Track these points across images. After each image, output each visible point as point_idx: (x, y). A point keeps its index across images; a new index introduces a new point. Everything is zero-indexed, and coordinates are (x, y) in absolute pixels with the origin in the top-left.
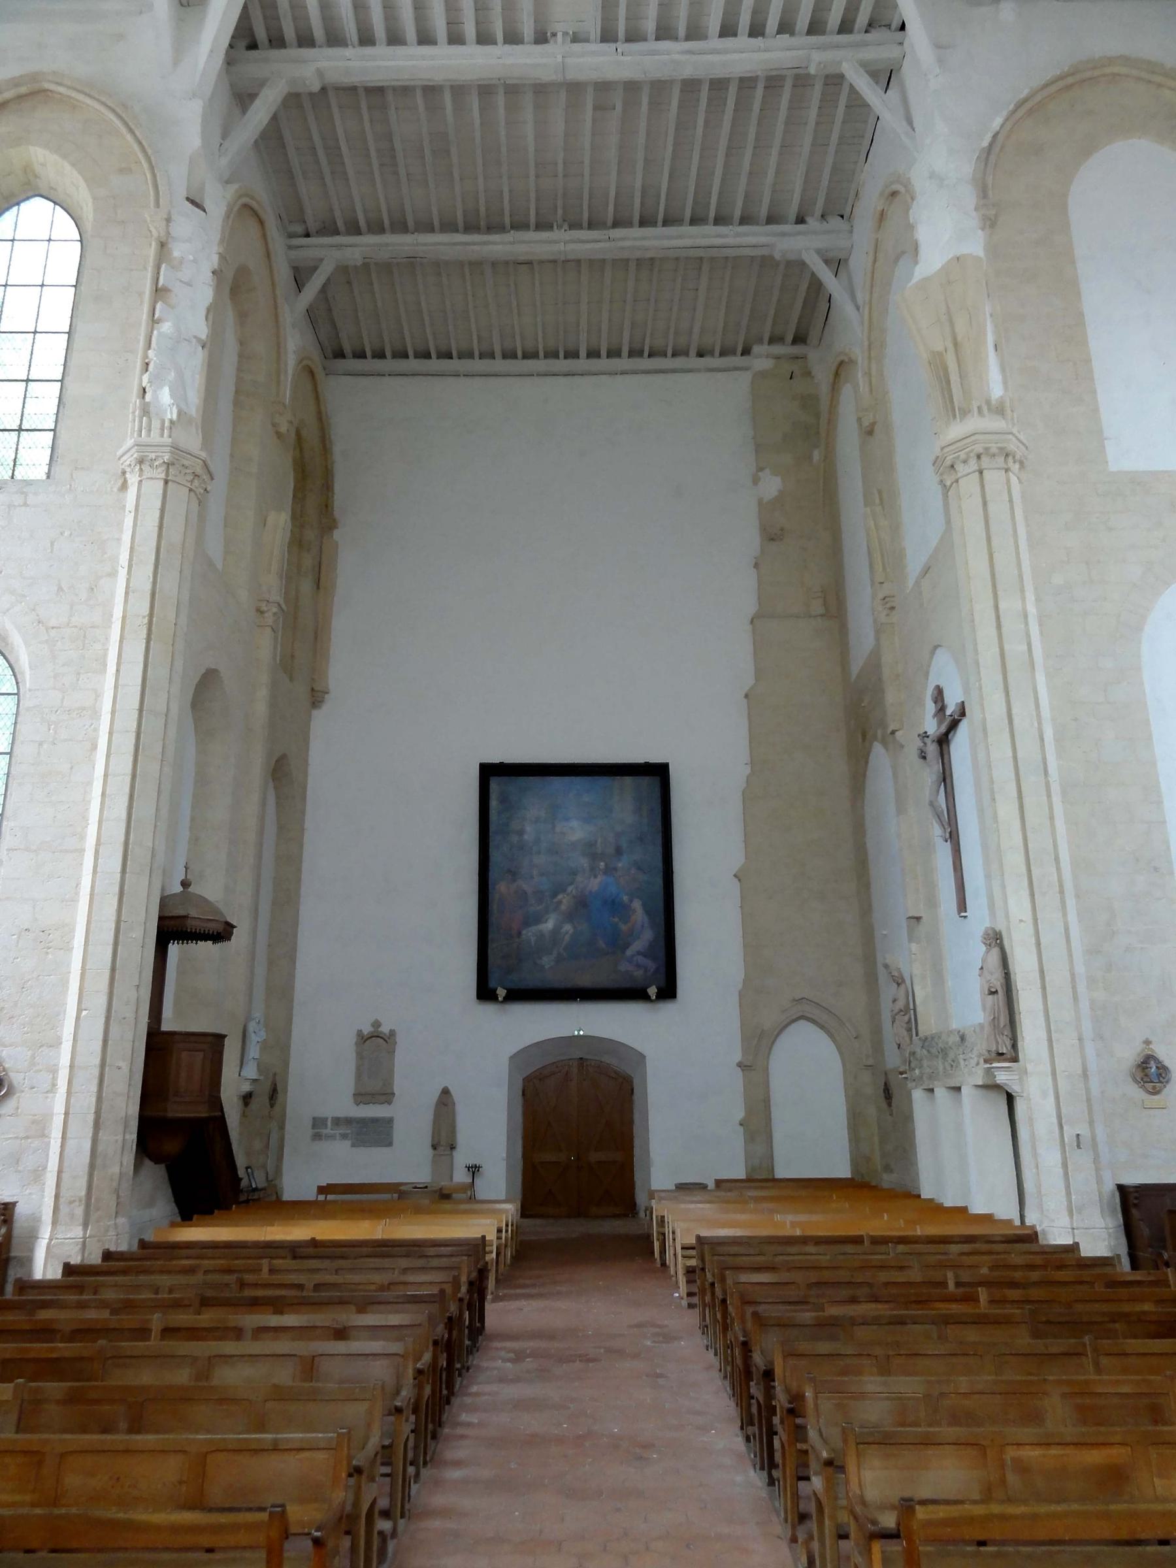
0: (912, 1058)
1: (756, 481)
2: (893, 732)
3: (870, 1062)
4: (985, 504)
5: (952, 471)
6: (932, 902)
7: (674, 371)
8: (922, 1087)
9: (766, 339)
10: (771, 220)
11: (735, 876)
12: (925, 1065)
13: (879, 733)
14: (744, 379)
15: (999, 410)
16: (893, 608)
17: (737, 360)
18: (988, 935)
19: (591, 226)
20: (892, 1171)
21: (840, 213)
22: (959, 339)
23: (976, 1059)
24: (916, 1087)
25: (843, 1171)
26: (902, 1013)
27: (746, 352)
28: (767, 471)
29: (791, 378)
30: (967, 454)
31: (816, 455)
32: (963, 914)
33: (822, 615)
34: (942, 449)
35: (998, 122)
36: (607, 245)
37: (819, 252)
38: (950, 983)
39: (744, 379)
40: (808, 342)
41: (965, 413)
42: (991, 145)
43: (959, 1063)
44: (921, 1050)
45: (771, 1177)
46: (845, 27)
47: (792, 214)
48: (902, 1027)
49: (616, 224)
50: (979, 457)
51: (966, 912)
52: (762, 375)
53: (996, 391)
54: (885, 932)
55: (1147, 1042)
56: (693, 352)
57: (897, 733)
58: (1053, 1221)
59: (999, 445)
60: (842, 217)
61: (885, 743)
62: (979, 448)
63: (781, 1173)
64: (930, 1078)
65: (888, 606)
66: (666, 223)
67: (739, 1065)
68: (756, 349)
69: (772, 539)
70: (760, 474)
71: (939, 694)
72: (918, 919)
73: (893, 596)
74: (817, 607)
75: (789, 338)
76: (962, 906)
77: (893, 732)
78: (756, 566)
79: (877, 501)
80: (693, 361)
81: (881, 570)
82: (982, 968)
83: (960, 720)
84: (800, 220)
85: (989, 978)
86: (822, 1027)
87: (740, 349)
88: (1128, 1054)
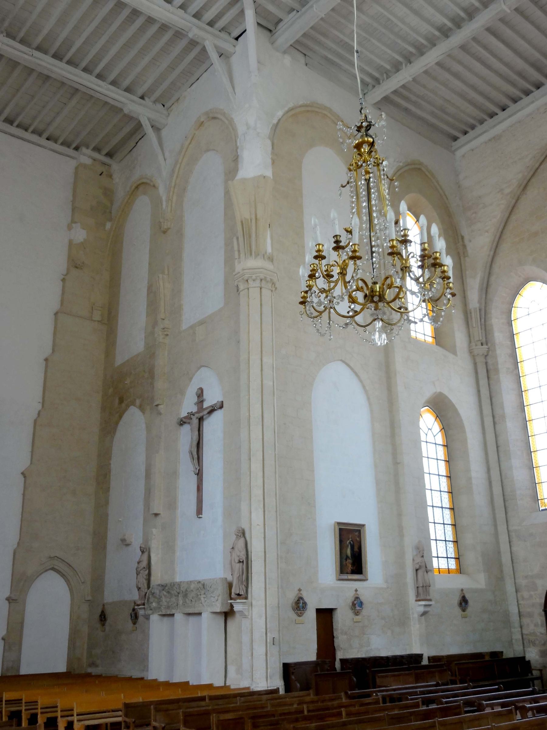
0: (151, 596)
1: (70, 228)
2: (157, 405)
3: (90, 598)
4: (261, 305)
5: (246, 283)
6: (172, 505)
7: (29, 141)
8: (160, 613)
9: (91, 147)
10: (128, 90)
11: (23, 473)
12: (164, 600)
13: (138, 402)
14: (73, 163)
15: (271, 259)
16: (167, 335)
17: (70, 151)
18: (240, 530)
19: (22, 42)
20: (97, 666)
21: (164, 104)
22: (258, 217)
23: (216, 597)
24: (153, 613)
25: (62, 668)
26: (145, 570)
27: (77, 149)
28: (79, 225)
29: (100, 175)
30: (256, 277)
31: (108, 225)
32: (200, 516)
33: (98, 321)
34: (243, 270)
35: (280, 113)
36: (30, 58)
37: (149, 119)
38: (178, 554)
39: (73, 163)
40: (114, 158)
41: (257, 255)
42: (278, 123)
43: (200, 599)
44: (160, 592)
45: (17, 674)
46: (211, 24)
47: (140, 92)
48: (143, 577)
49: (39, 48)
50: (261, 280)
51: (202, 515)
52: (85, 166)
53: (269, 250)
54: (120, 520)
55: (300, 590)
56: (45, 135)
57: (160, 407)
58: (258, 684)
59: (271, 277)
60: (164, 106)
61: (141, 408)
62: (262, 276)
63: (23, 671)
64: (168, 607)
65: (166, 333)
66: (69, 62)
67: (8, 599)
68: (84, 150)
69: (77, 267)
70: (74, 225)
71: (200, 394)
72: (156, 515)
73: (169, 329)
74: (97, 316)
75: (105, 152)
76: (199, 511)
77: (157, 405)
78: (63, 280)
79: (166, 272)
80: (43, 141)
81: (163, 311)
82: (233, 548)
83: (216, 410)
84: (142, 98)
85: (238, 554)
86: (63, 575)
87: (74, 146)
88: (292, 596)
